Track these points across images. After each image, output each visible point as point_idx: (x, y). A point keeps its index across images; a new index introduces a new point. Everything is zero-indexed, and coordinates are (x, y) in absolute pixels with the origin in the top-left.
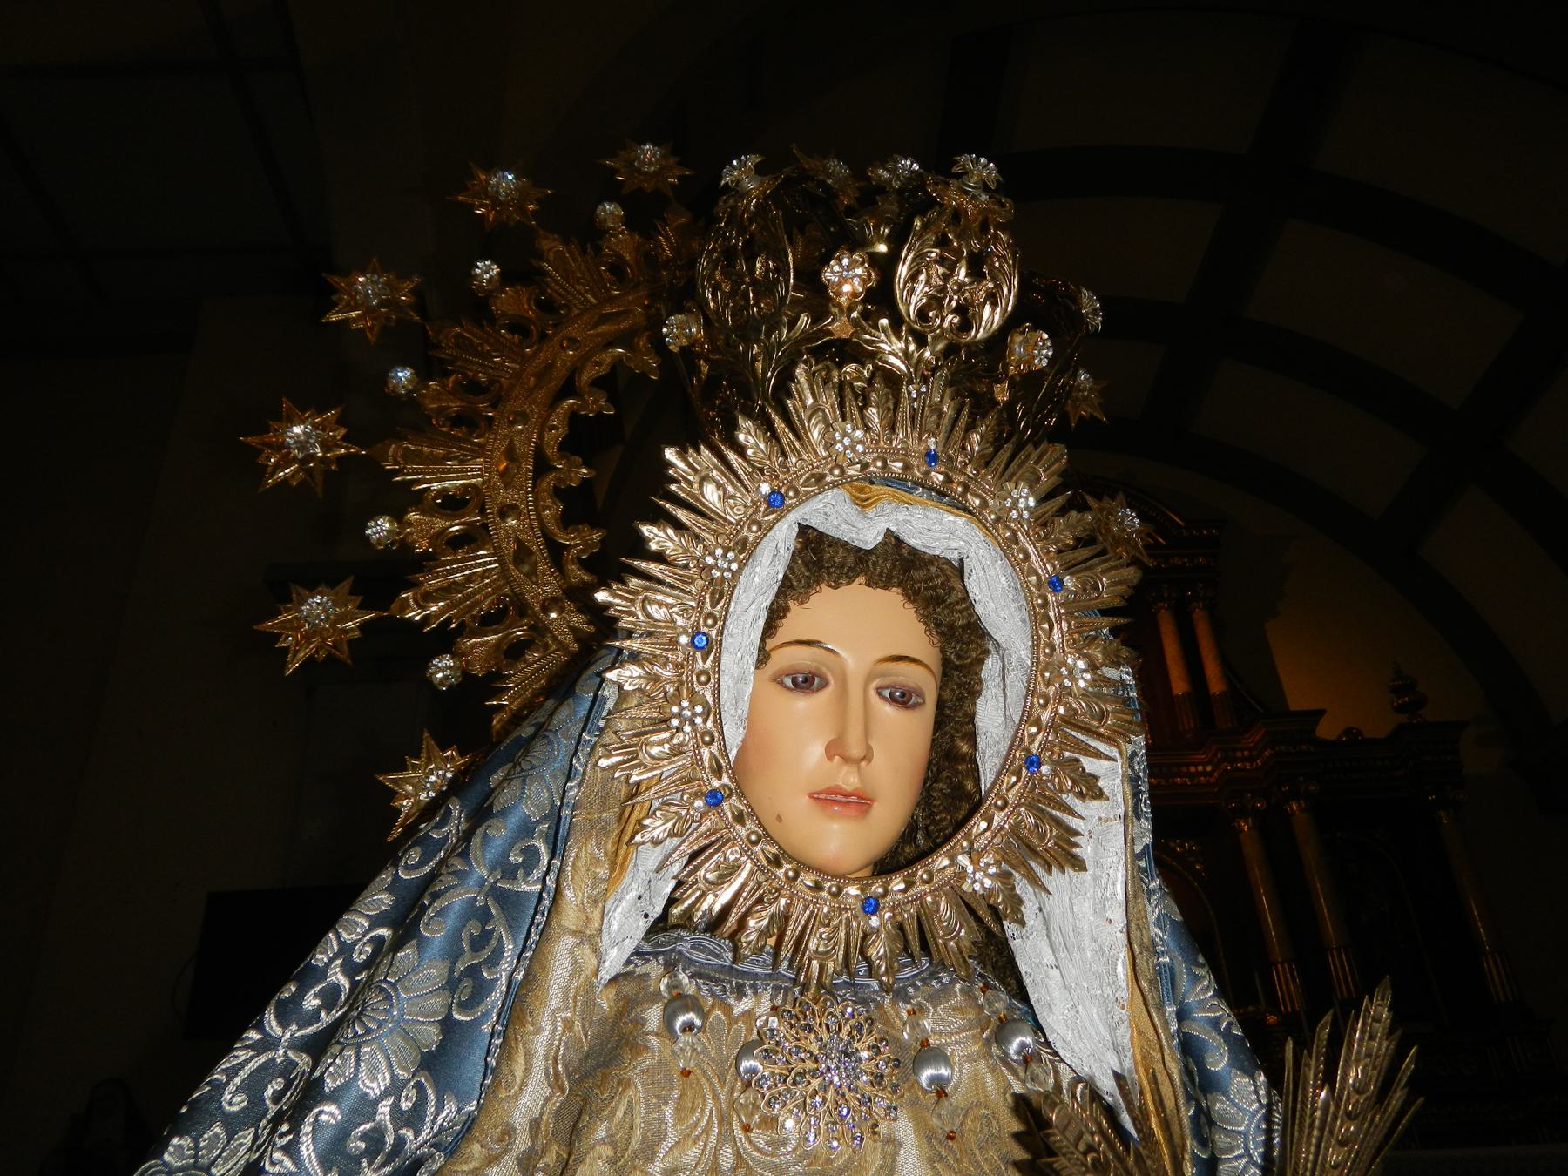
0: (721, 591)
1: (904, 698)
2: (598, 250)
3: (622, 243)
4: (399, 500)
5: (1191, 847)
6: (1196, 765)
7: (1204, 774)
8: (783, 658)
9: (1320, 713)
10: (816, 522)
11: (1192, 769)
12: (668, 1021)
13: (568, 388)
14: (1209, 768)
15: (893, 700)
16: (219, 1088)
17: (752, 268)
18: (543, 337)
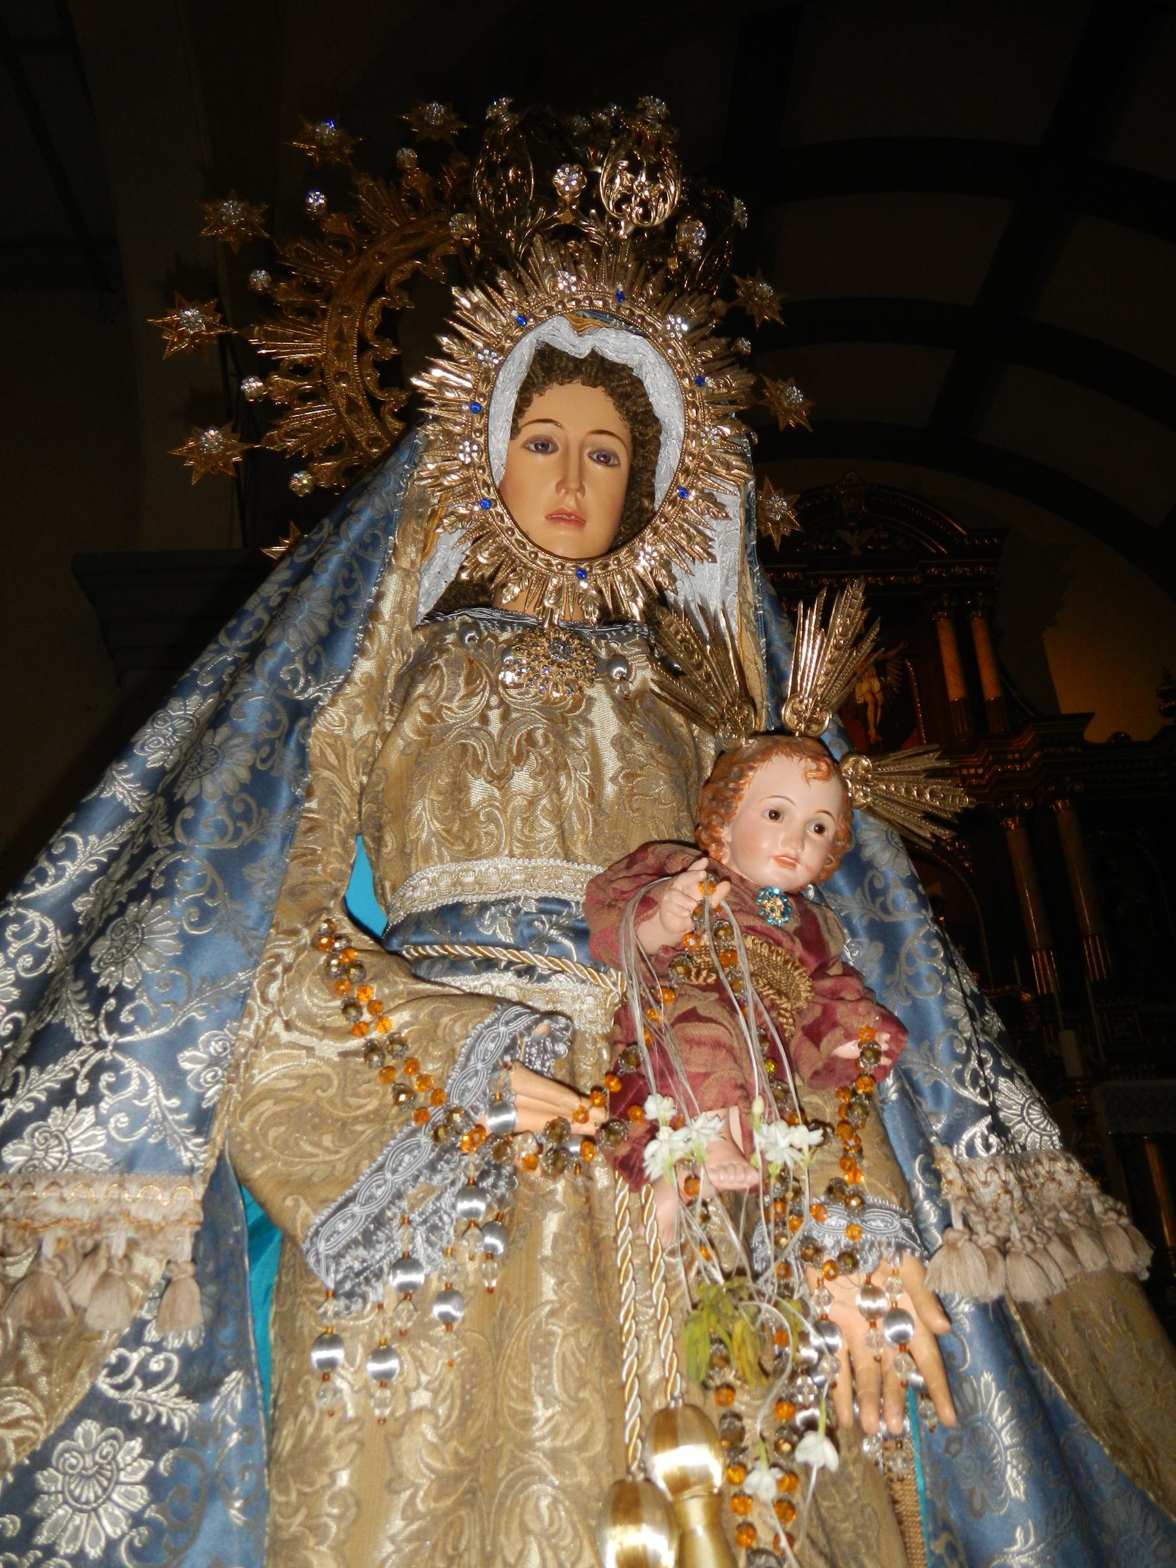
0: (487, 377)
1: (605, 458)
2: (399, 185)
3: (416, 180)
4: (265, 367)
6: (968, 768)
7: (976, 776)
8: (529, 432)
9: (1089, 716)
11: (965, 772)
13: (379, 290)
14: (980, 771)
15: (598, 461)
16: (196, 675)
17: (507, 177)
18: (360, 251)
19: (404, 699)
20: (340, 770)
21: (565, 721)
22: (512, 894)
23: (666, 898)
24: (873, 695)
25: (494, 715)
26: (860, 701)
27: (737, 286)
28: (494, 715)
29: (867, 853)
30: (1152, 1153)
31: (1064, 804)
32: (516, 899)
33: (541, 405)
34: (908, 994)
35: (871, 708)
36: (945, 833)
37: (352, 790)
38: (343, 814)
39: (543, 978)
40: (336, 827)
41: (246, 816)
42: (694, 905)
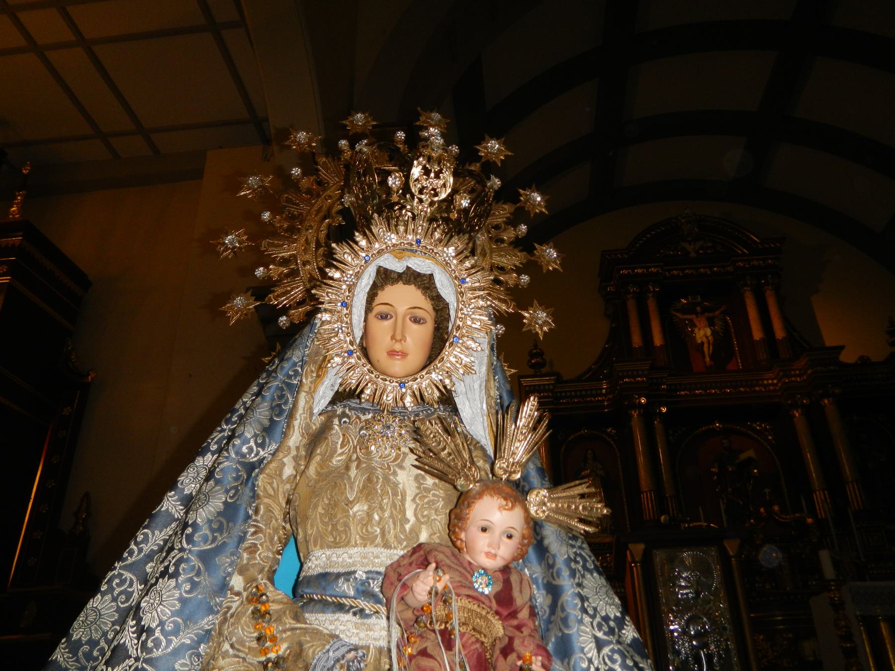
1: (417, 320)
2: (339, 159)
5: (765, 427)
6: (768, 380)
7: (773, 384)
8: (377, 309)
9: (841, 348)
10: (382, 264)
11: (765, 382)
12: (340, 422)
14: (775, 381)
16: (209, 444)
17: (365, 179)
19: (310, 455)
20: (274, 497)
21: (389, 468)
22: (353, 569)
23: (414, 585)
24: (707, 337)
25: (354, 465)
26: (699, 341)
27: (521, 195)
29: (546, 542)
30: (884, 627)
32: (355, 572)
34: (560, 630)
35: (706, 345)
37: (281, 506)
38: (274, 521)
39: (368, 616)
40: (268, 531)
41: (220, 530)
42: (429, 588)
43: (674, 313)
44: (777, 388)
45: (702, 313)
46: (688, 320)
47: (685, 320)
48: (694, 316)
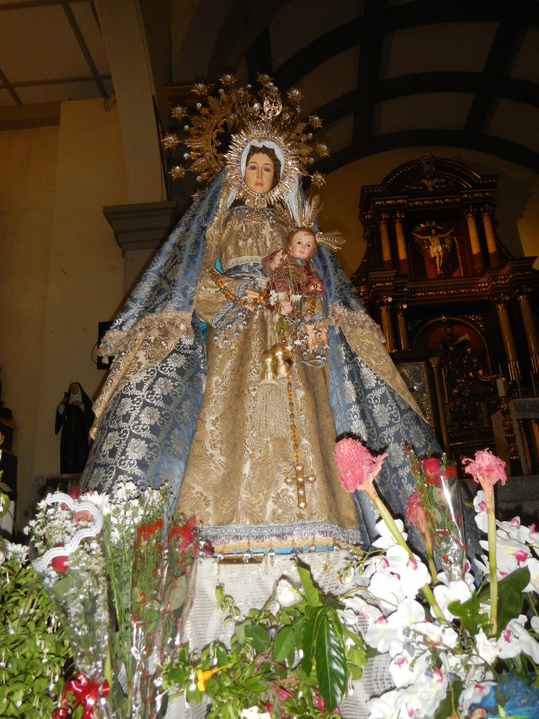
0: (240, 154)
1: (267, 170)
2: (220, 99)
3: (224, 97)
4: (189, 150)
5: (478, 318)
6: (481, 283)
7: (485, 287)
8: (250, 165)
9: (535, 258)
10: (253, 144)
11: (479, 285)
13: (216, 128)
14: (486, 284)
15: (266, 171)
18: (211, 118)
19: (225, 225)
20: (213, 241)
24: (439, 253)
25: (244, 228)
26: (433, 256)
27: (309, 118)
28: (244, 228)
31: (523, 297)
33: (253, 159)
35: (438, 259)
36: (339, 248)
41: (194, 249)
43: (415, 235)
44: (488, 289)
45: (436, 234)
46: (425, 240)
47: (423, 240)
48: (429, 237)
